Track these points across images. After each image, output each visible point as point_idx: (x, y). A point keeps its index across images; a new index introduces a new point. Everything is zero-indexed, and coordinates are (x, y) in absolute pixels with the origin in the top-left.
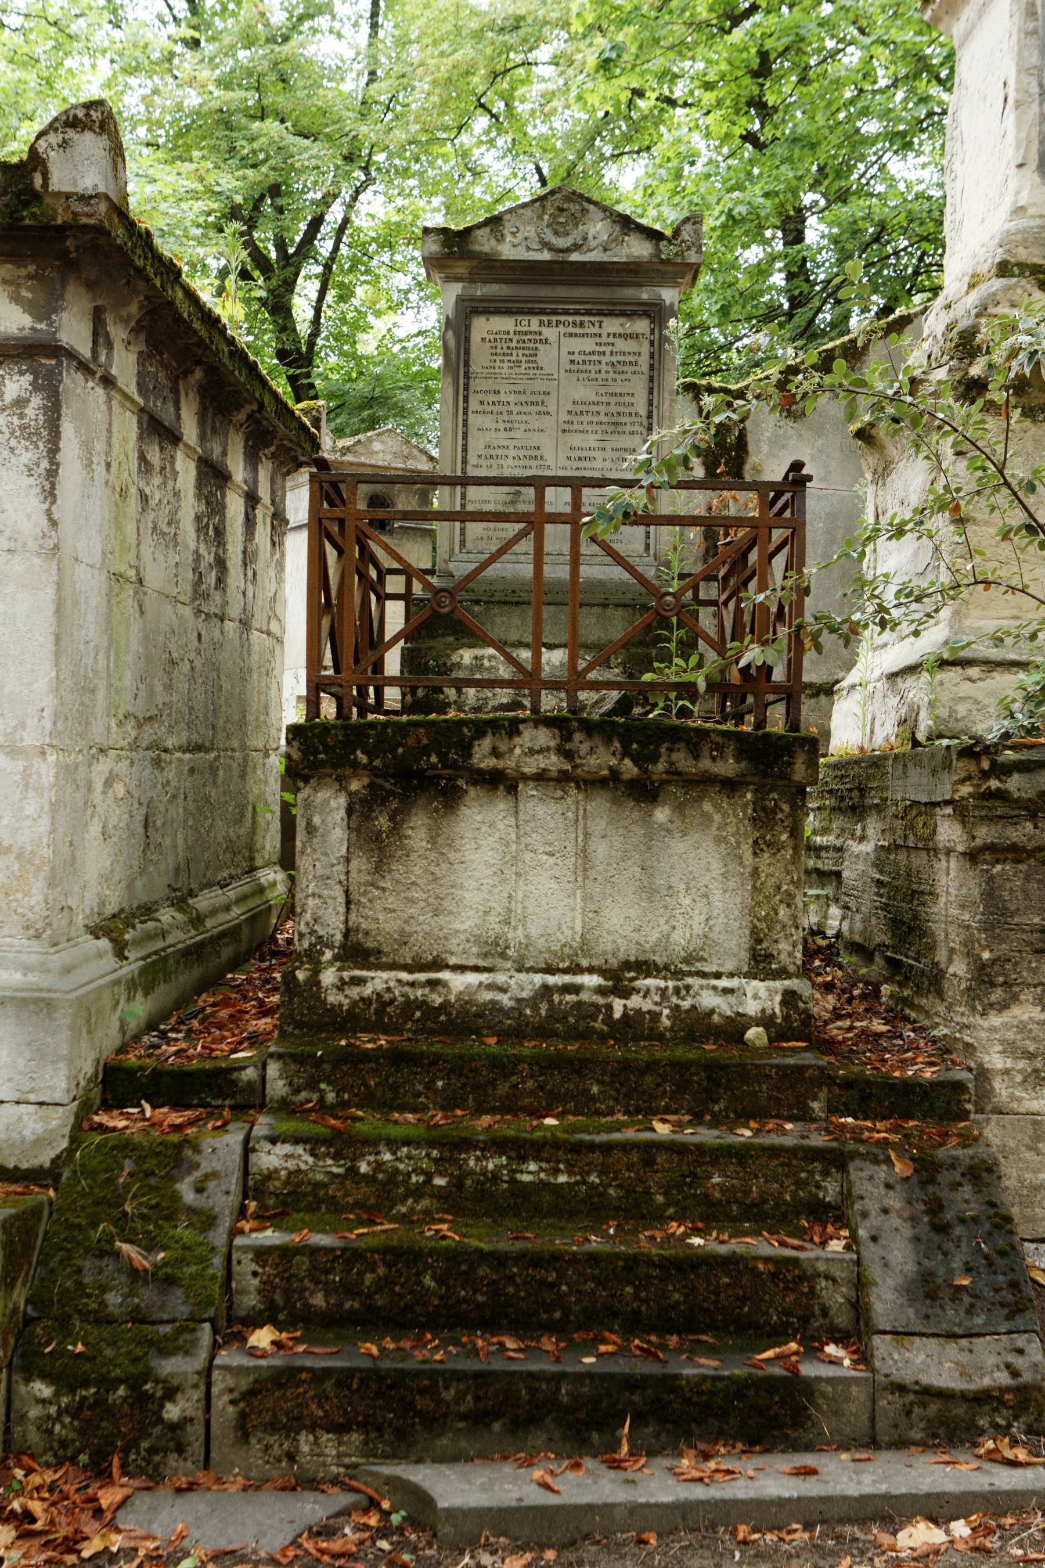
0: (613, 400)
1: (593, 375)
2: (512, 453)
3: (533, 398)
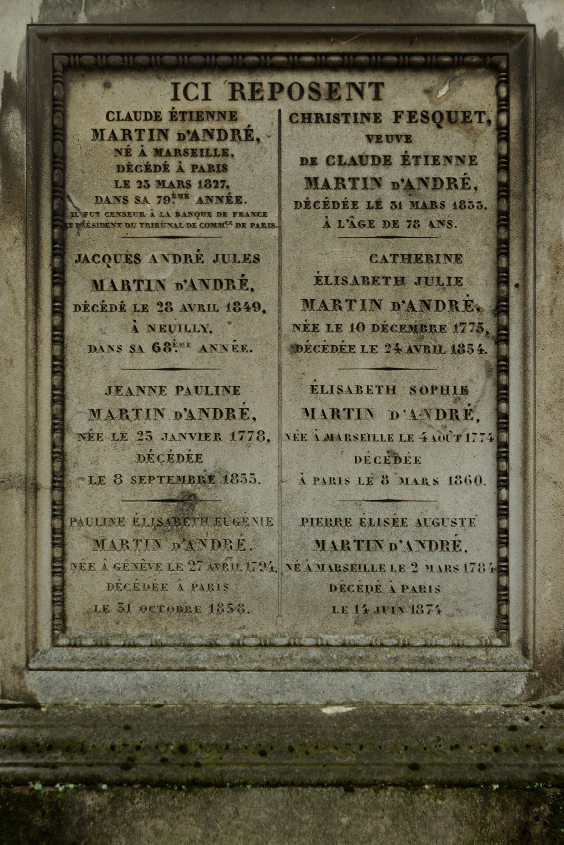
0: (411, 272)
1: (362, 214)
2: (173, 403)
3: (220, 272)
